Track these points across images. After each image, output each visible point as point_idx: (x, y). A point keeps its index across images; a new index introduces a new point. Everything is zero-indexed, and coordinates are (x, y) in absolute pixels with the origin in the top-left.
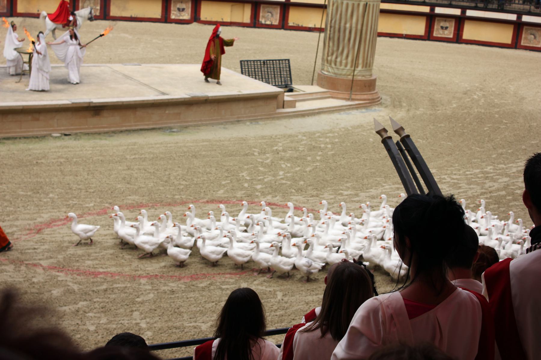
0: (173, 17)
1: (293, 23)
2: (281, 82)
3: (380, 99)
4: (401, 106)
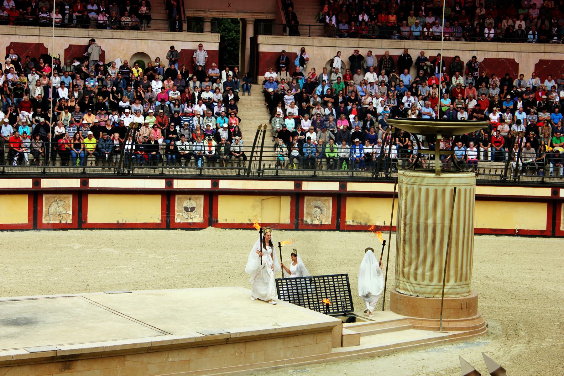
0: (178, 220)
2: (338, 307)
3: (485, 326)
4: (518, 336)
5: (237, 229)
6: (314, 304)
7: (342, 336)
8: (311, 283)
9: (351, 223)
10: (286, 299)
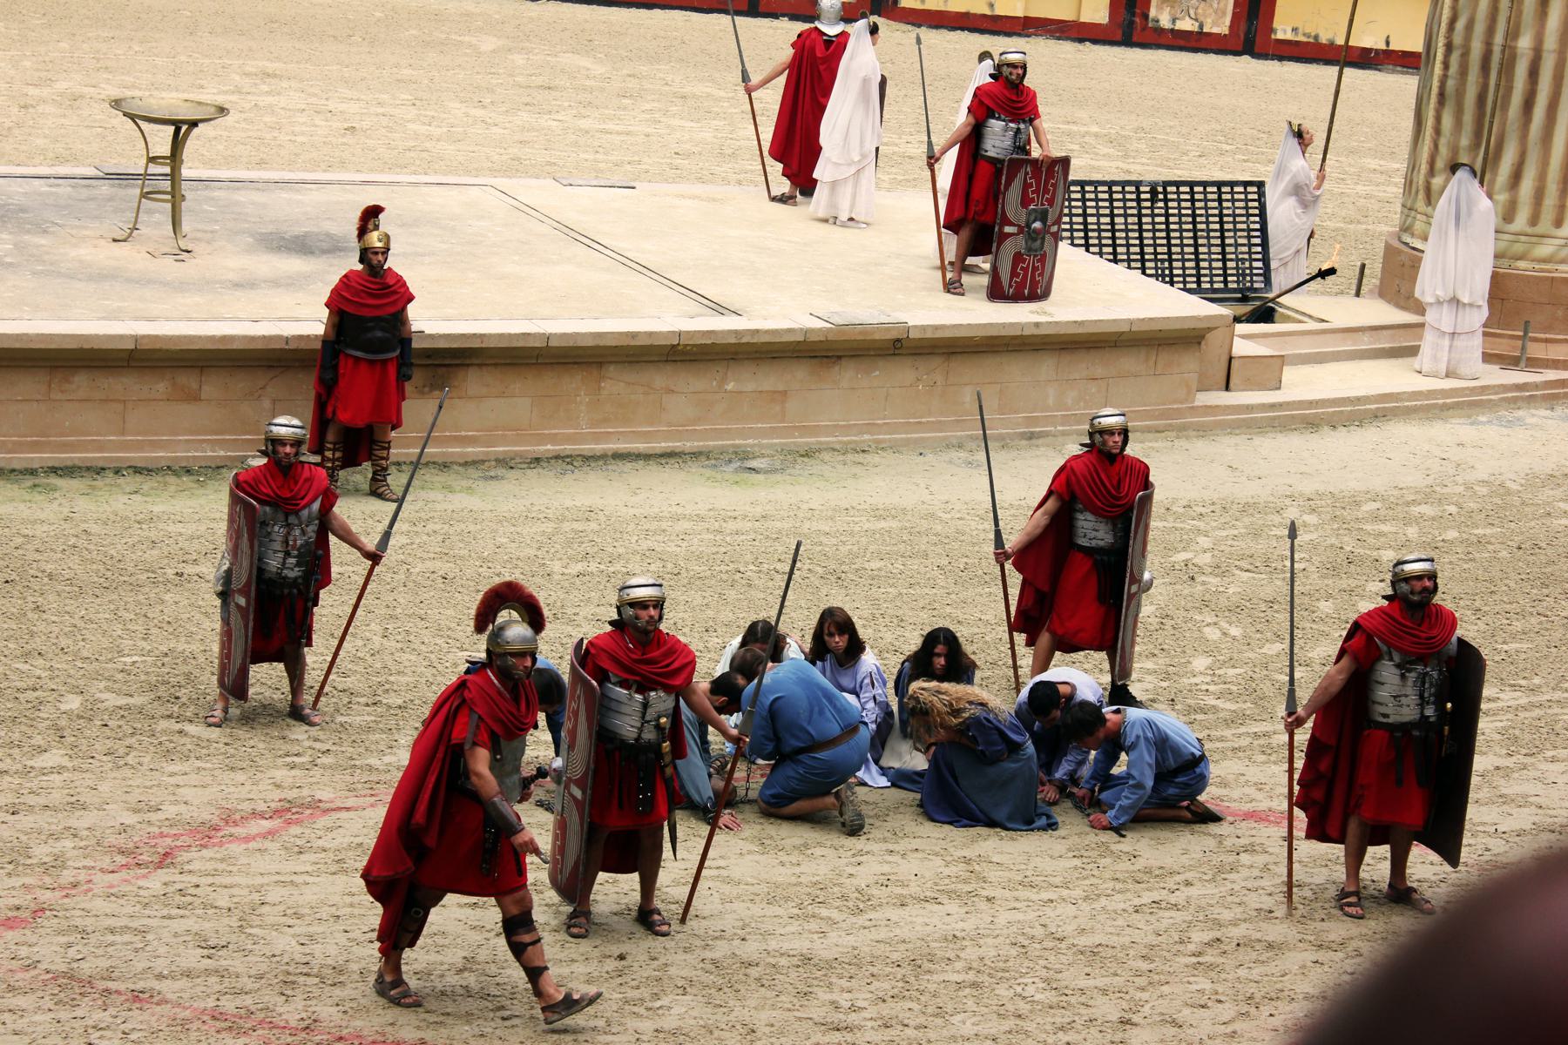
1: (1295, 30)
2: (1225, 275)
5: (953, 28)
6: (1156, 260)
7: (1231, 359)
8: (1153, 200)
9: (1289, 36)
10: (1076, 242)
